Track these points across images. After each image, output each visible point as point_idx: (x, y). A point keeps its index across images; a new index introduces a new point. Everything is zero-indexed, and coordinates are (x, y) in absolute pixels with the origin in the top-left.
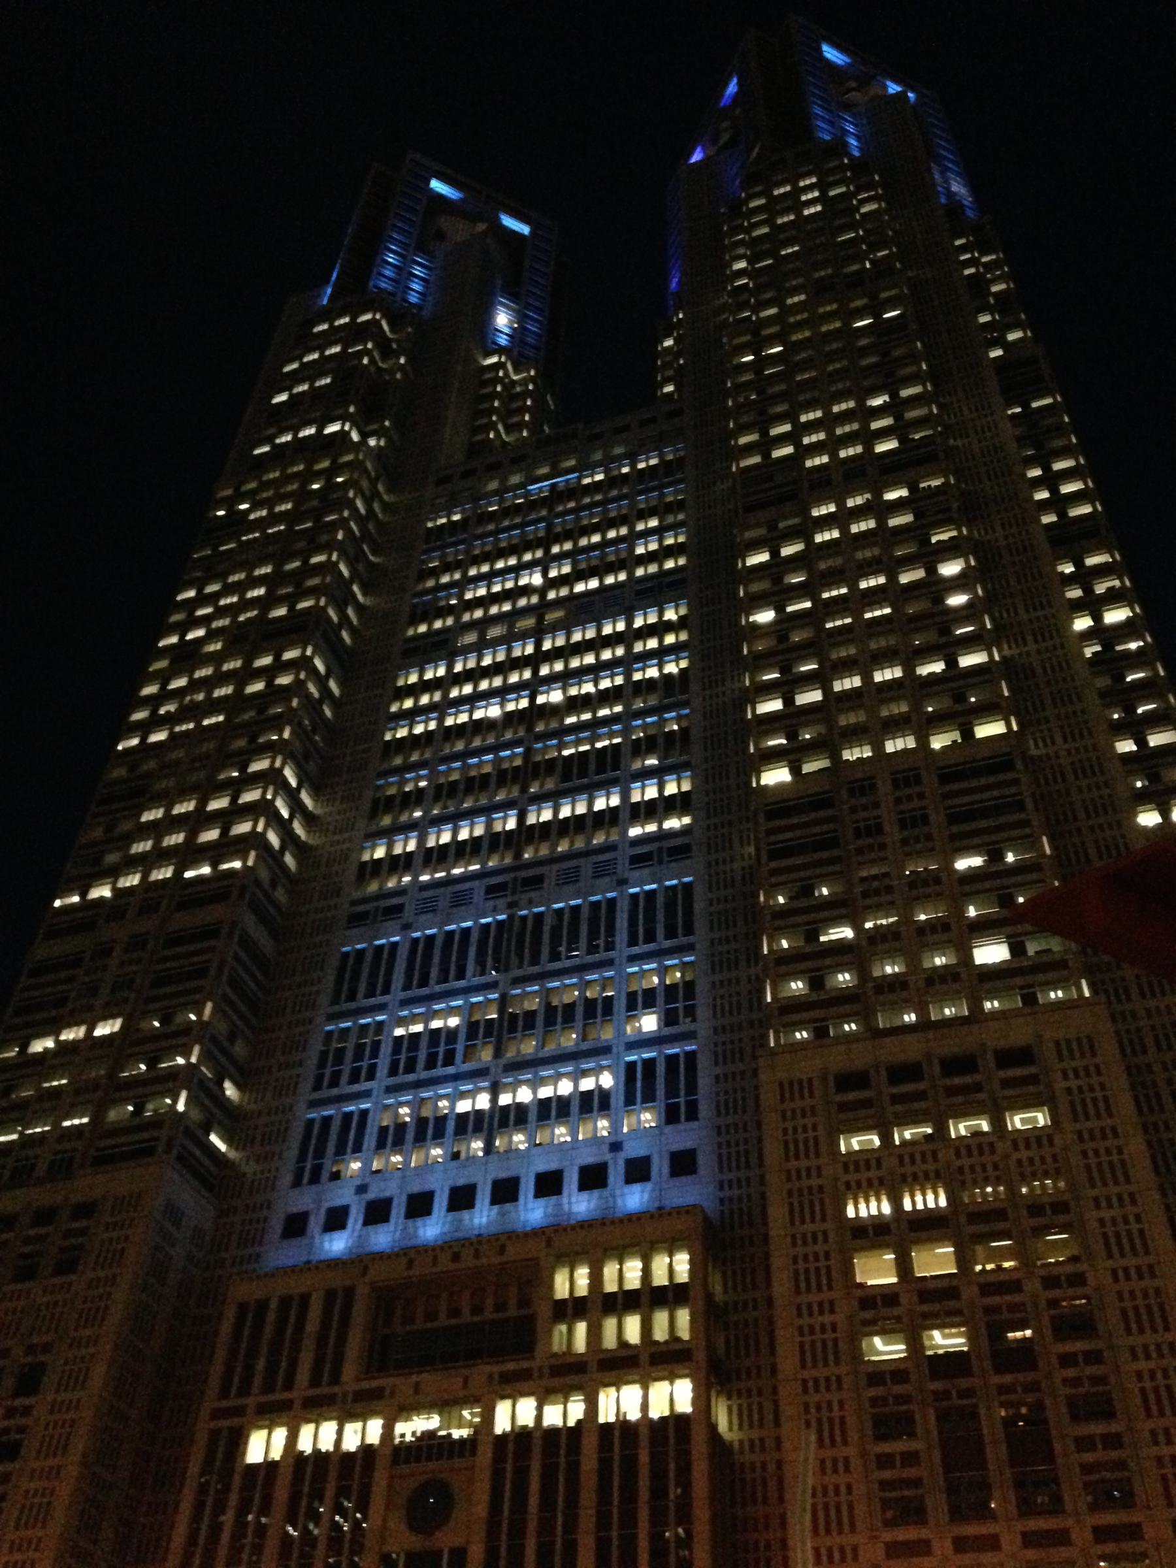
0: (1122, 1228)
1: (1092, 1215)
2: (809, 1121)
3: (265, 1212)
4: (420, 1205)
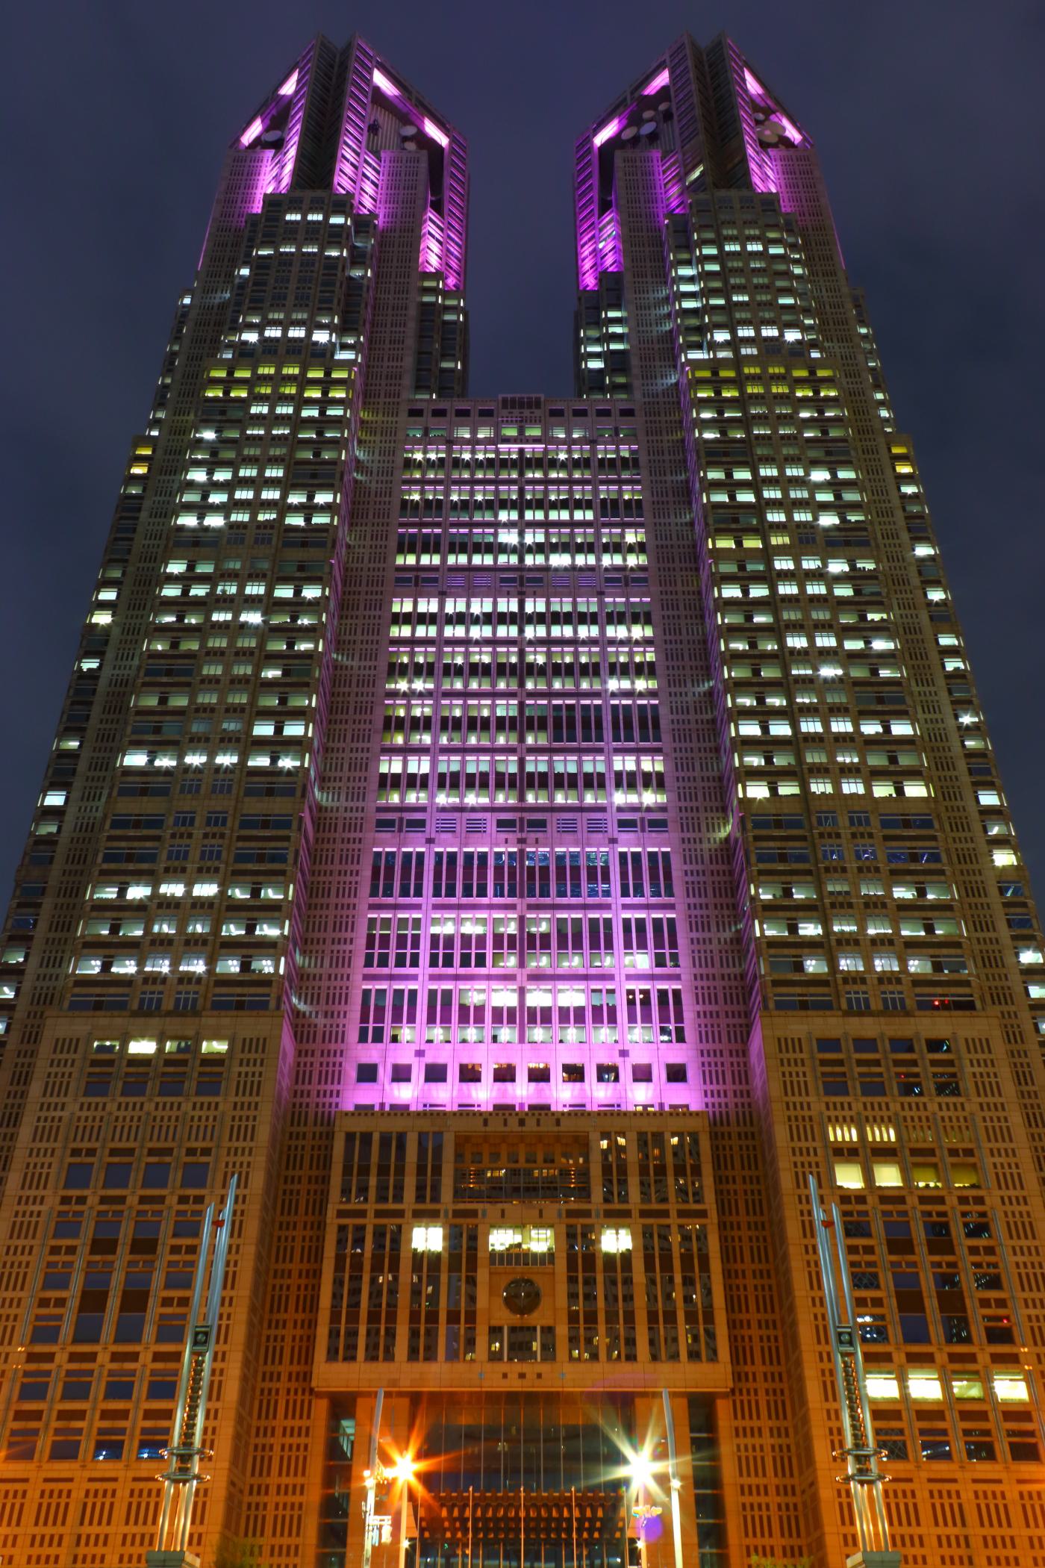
0: (1007, 1171)
1: (989, 1161)
2: (800, 1069)
3: (338, 1059)
4: (470, 1074)
